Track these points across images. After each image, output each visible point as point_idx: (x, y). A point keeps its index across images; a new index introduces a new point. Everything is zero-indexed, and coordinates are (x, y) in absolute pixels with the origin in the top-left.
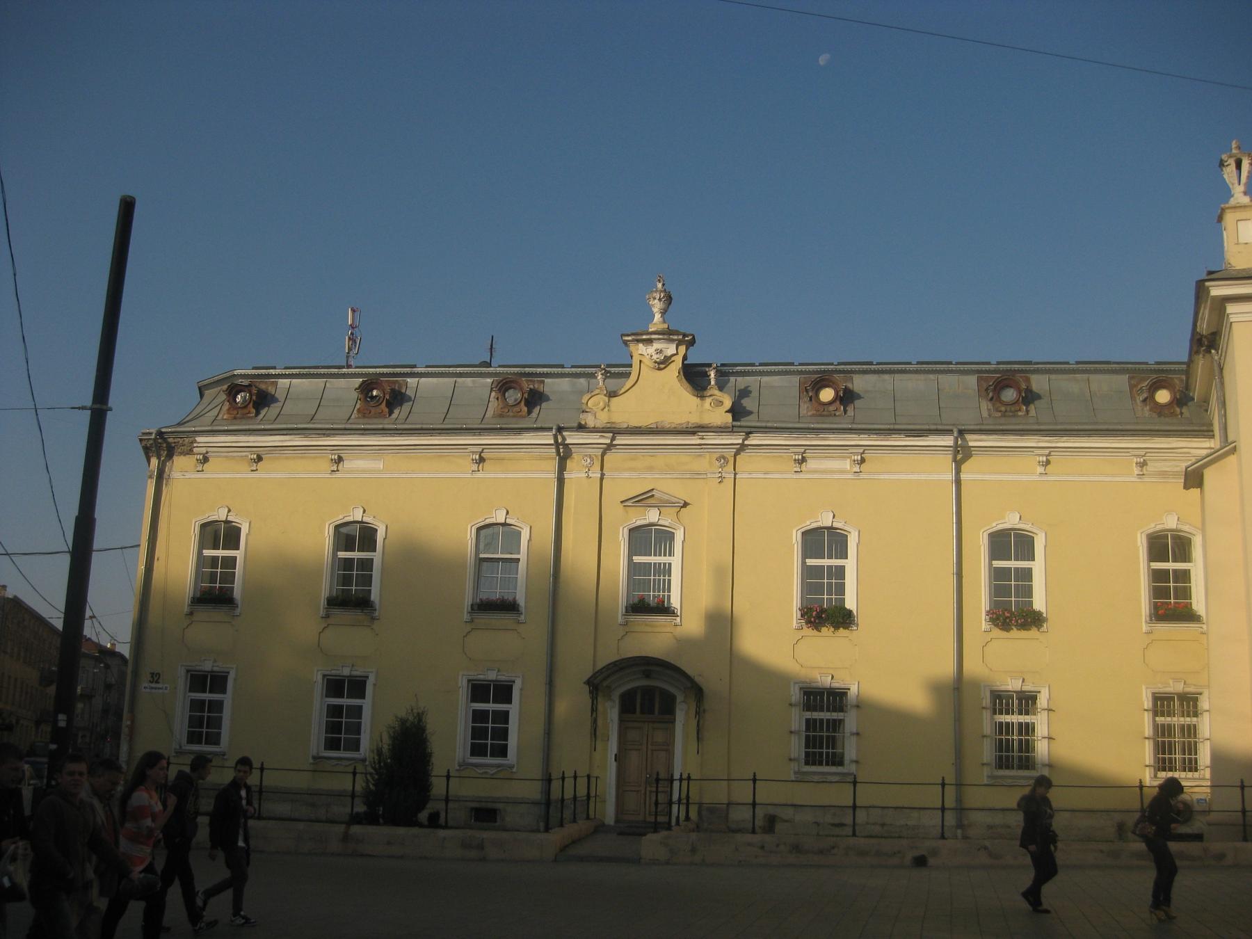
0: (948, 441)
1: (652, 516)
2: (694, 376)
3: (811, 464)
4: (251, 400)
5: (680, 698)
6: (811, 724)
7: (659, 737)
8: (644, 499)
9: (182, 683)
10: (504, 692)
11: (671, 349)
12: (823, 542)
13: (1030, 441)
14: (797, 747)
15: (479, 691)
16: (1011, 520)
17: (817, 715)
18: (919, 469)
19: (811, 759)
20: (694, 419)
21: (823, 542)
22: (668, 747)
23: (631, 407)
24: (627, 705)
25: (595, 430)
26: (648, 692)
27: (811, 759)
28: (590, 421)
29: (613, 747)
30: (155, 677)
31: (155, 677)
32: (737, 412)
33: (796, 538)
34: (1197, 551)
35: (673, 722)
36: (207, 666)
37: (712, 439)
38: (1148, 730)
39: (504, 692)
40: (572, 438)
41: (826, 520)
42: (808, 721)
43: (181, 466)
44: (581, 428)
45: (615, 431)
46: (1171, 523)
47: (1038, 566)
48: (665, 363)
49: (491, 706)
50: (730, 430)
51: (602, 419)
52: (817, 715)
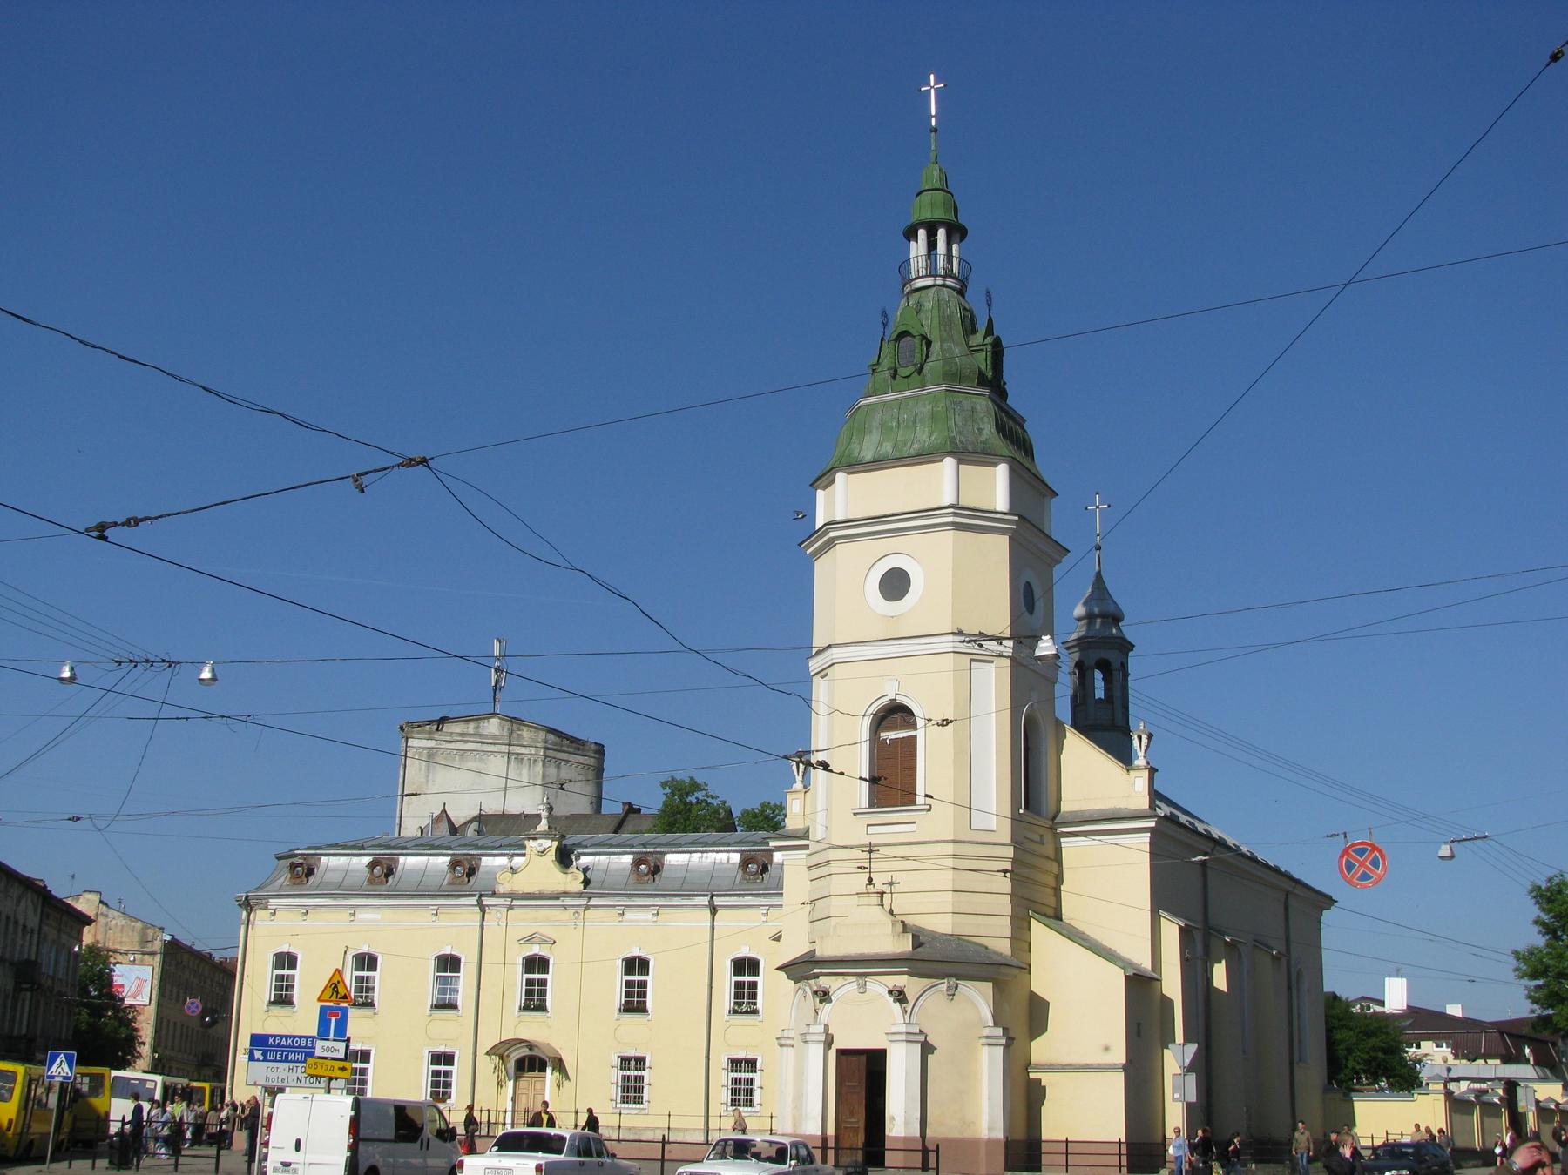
1: (535, 950)
2: (564, 858)
4: (302, 871)
8: (529, 940)
10: (449, 1059)
11: (548, 843)
15: (436, 1058)
16: (745, 952)
18: (689, 920)
19: (625, 1100)
20: (562, 888)
23: (521, 884)
25: (504, 896)
26: (532, 1059)
27: (625, 1100)
28: (501, 889)
32: (586, 882)
37: (568, 902)
39: (449, 1059)
40: (486, 901)
42: (624, 1077)
43: (260, 916)
44: (494, 894)
45: (513, 896)
48: (542, 853)
49: (442, 1068)
50: (579, 895)
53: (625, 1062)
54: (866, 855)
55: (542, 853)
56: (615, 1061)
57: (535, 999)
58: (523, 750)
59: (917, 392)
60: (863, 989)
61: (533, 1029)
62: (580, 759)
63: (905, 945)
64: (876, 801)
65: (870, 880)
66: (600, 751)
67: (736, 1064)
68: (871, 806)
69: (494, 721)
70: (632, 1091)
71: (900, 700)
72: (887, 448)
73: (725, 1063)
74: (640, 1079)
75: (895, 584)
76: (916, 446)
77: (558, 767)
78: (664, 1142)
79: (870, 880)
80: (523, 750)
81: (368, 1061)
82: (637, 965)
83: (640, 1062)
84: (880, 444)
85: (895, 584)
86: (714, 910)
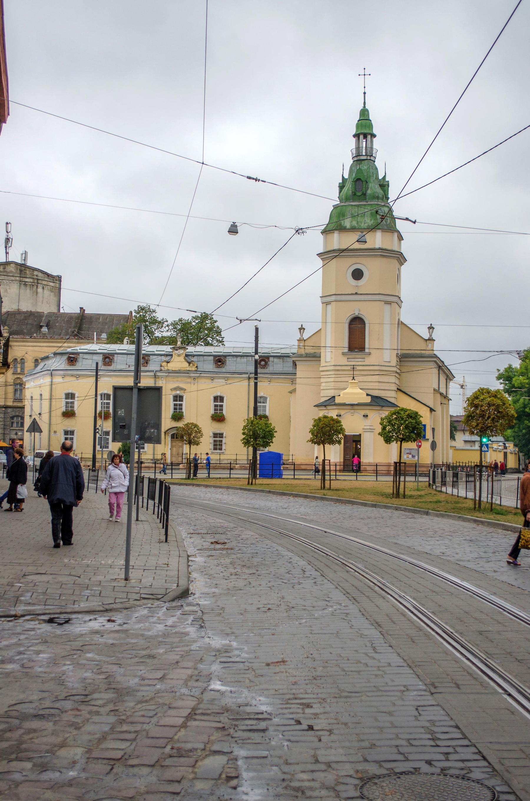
1: (178, 392)
6: (215, 441)
7: (180, 444)
8: (176, 389)
9: (63, 433)
12: (218, 399)
14: (212, 447)
17: (216, 439)
19: (215, 449)
24: (173, 436)
27: (215, 449)
29: (170, 447)
30: (55, 432)
31: (55, 432)
36: (69, 429)
40: (158, 374)
41: (219, 394)
45: (169, 372)
47: (267, 405)
51: (166, 368)
52: (216, 439)
55: (179, 355)
56: (211, 434)
58: (27, 280)
59: (365, 203)
62: (52, 284)
63: (368, 400)
64: (351, 348)
66: (59, 279)
69: (13, 265)
71: (360, 316)
72: (354, 223)
74: (221, 441)
75: (358, 274)
76: (366, 225)
77: (43, 288)
78: (231, 464)
80: (27, 280)
81: (73, 435)
82: (218, 399)
84: (352, 222)
85: (358, 274)
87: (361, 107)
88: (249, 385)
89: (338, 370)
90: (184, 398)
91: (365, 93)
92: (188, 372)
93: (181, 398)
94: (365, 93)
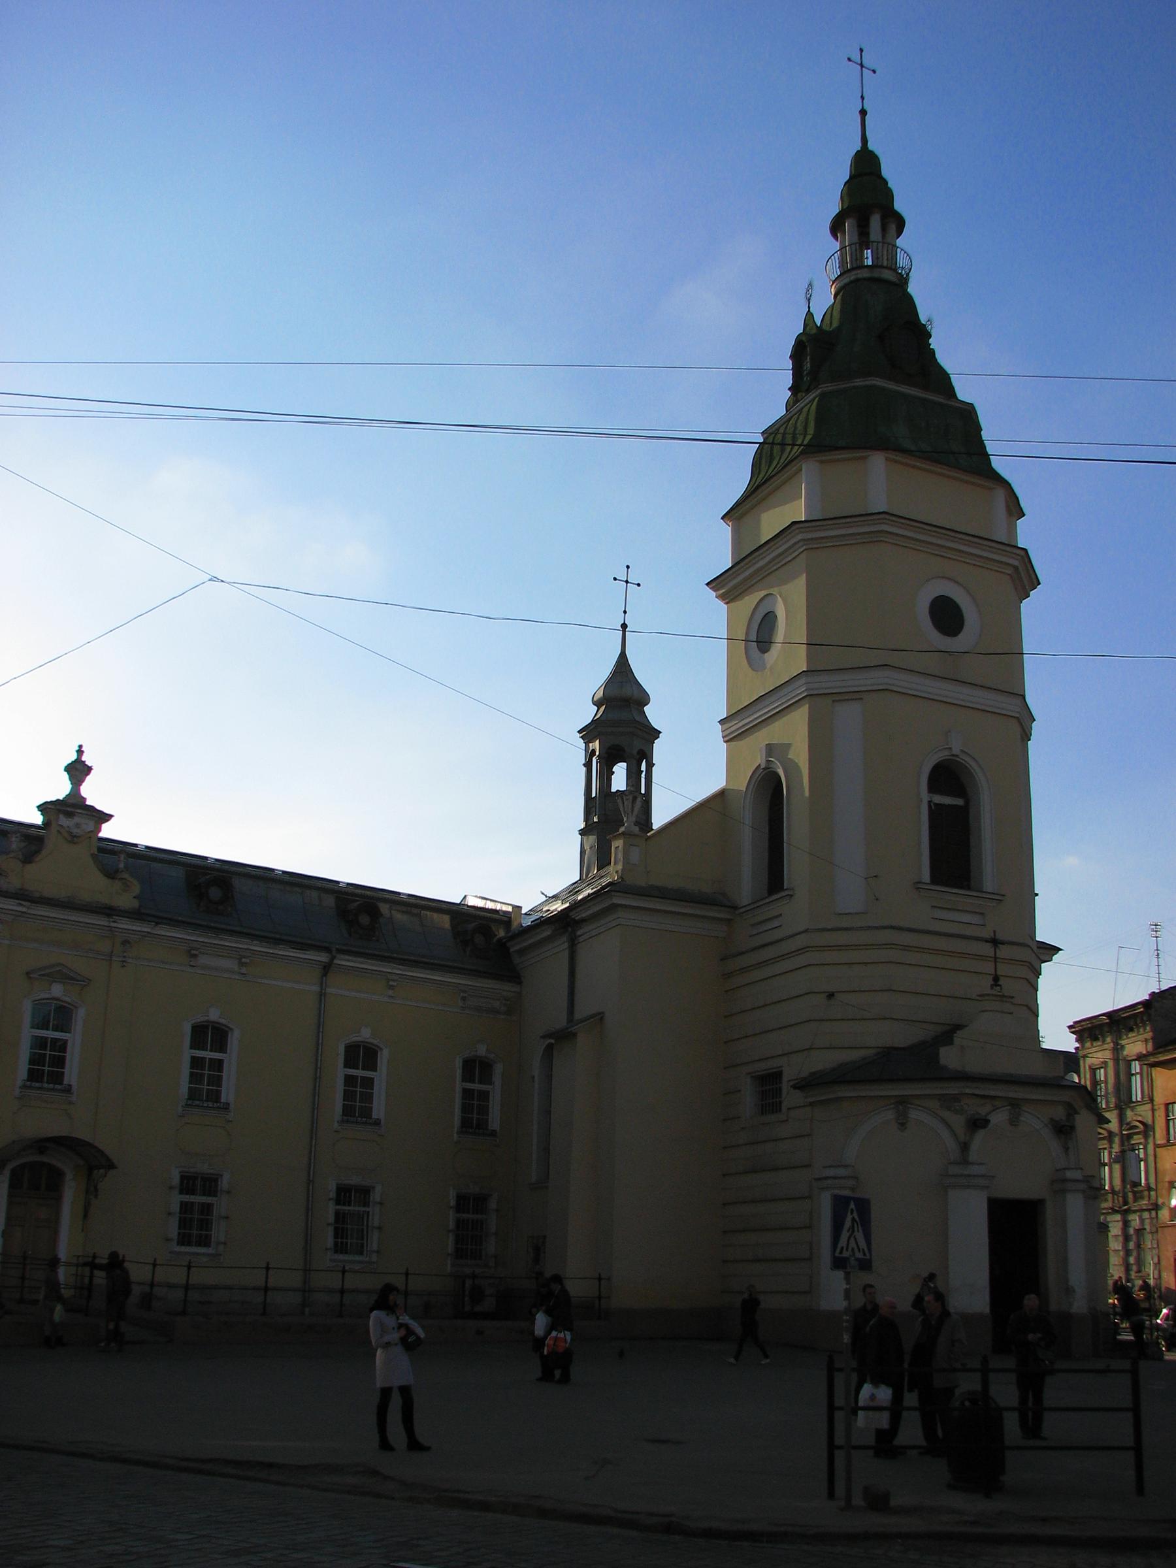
0: (323, 957)
1: (57, 990)
3: (203, 960)
5: (69, 1176)
13: (386, 968)
16: (366, 1035)
21: (210, 1035)
22: (53, 1225)
27: (184, 1240)
33: (187, 1029)
34: (497, 1078)
35: (59, 1199)
38: (452, 1225)
42: (182, 1203)
46: (482, 1050)
53: (189, 1183)
54: (988, 949)
56: (176, 1181)
57: (47, 1067)
60: (1014, 1121)
61: (44, 1119)
65: (996, 979)
67: (344, 1194)
68: (935, 879)
70: (195, 1226)
73: (333, 1195)
79: (996, 979)
83: (210, 1184)
86: (326, 968)
87: (858, 146)
88: (322, 995)
89: (906, 948)
90: (80, 1015)
91: (863, 113)
92: (109, 911)
93: (62, 1016)
94: (863, 113)
